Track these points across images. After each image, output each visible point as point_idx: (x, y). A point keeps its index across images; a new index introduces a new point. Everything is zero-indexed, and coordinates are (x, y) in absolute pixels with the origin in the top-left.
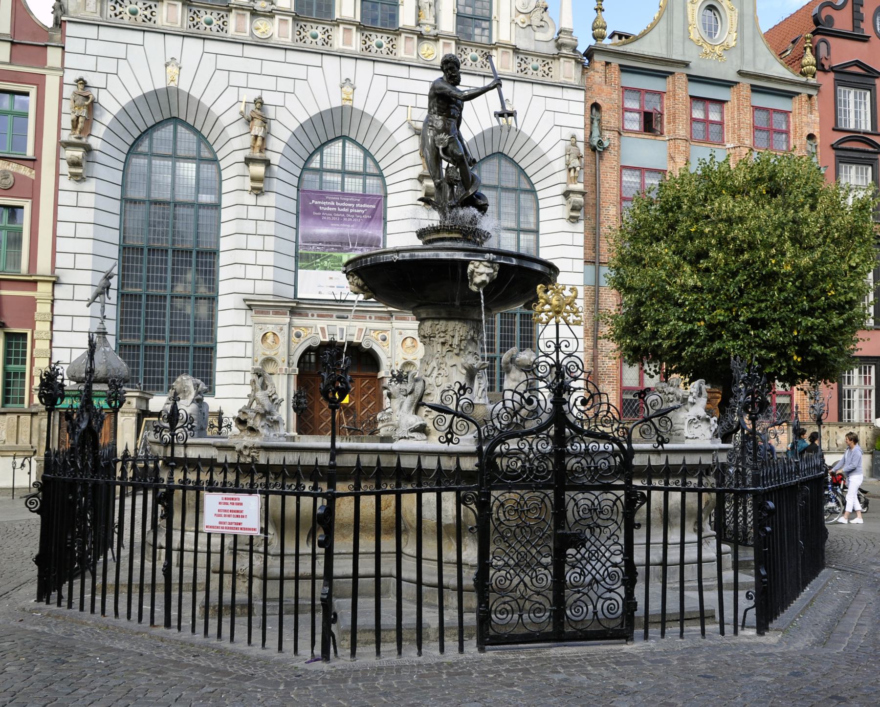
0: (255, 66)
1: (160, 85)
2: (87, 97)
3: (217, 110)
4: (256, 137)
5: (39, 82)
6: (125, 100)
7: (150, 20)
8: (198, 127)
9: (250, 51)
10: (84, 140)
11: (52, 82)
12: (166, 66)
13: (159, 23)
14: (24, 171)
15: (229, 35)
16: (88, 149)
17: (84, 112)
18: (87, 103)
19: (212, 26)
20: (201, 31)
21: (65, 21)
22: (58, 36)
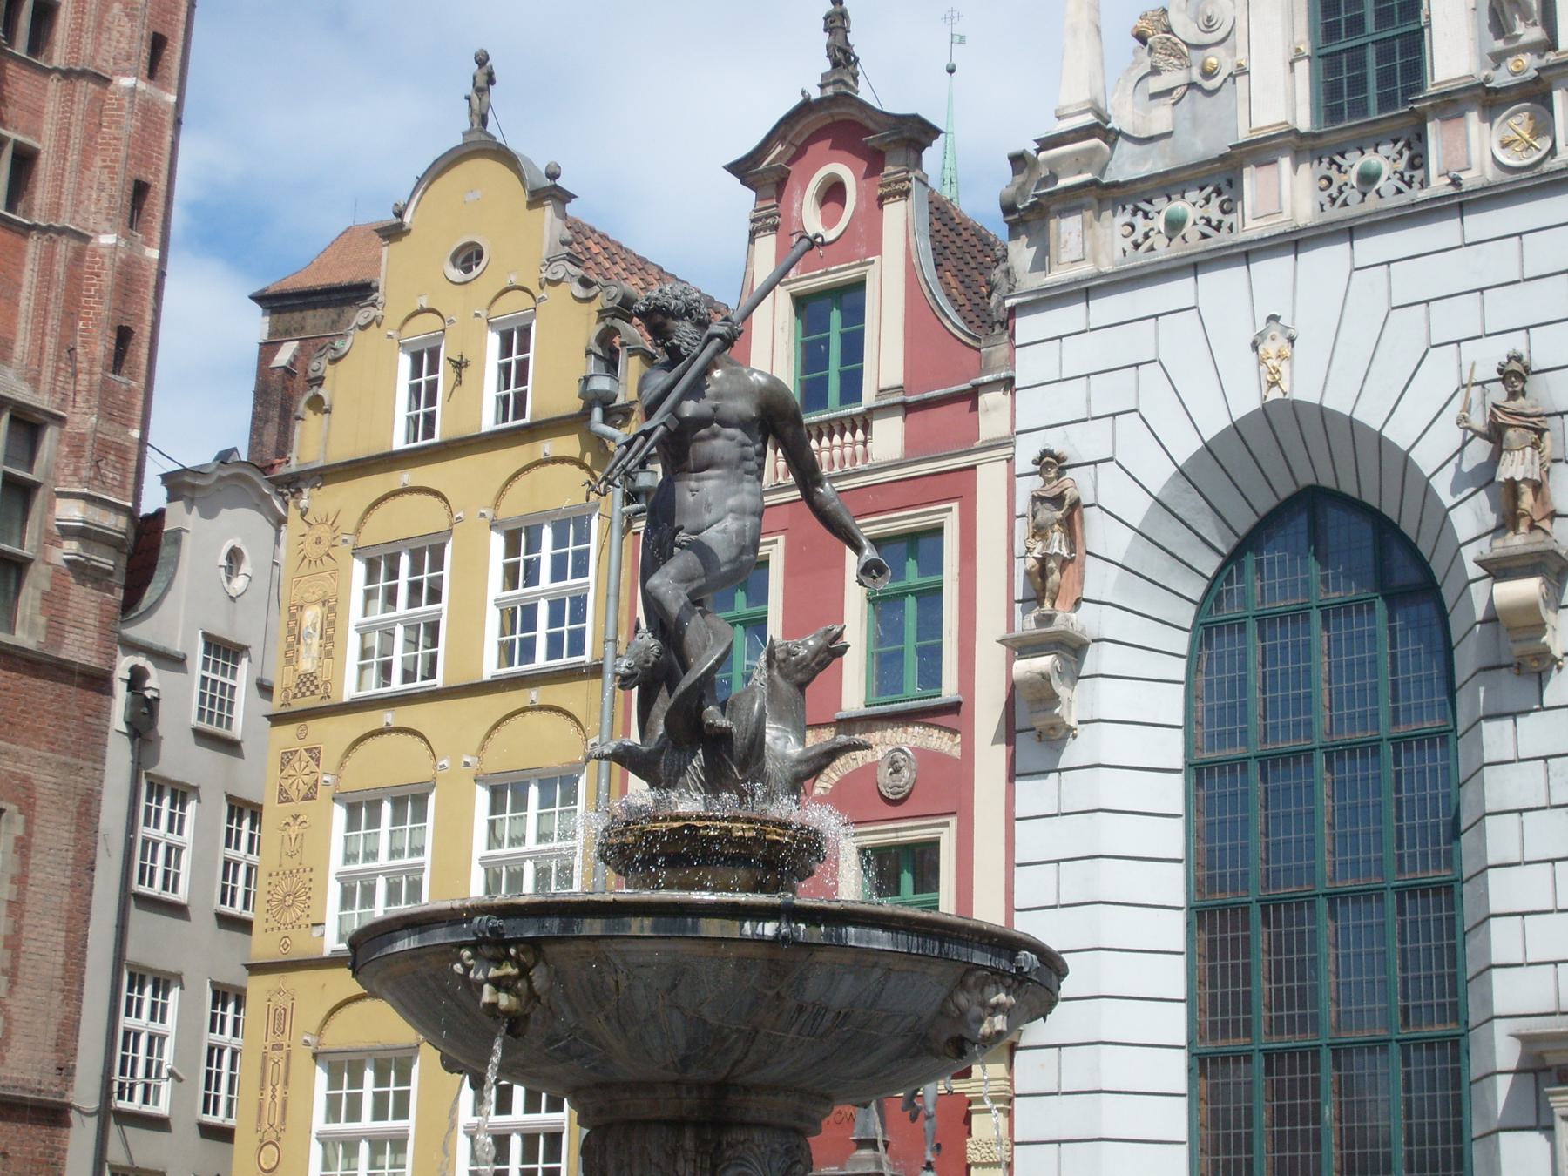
0: (1500, 262)
1: (1246, 402)
2: (1058, 500)
3: (1399, 434)
4: (1513, 486)
5: (960, 487)
6: (1159, 475)
7: (1218, 229)
8: (1371, 499)
9: (1480, 224)
10: (1059, 624)
11: (990, 480)
12: (1255, 346)
13: (1237, 225)
14: (939, 741)
15: (1423, 195)
16: (1072, 649)
17: (1057, 544)
18: (1059, 515)
19: (1381, 183)
20: (1355, 209)
21: (1012, 312)
22: (999, 352)
